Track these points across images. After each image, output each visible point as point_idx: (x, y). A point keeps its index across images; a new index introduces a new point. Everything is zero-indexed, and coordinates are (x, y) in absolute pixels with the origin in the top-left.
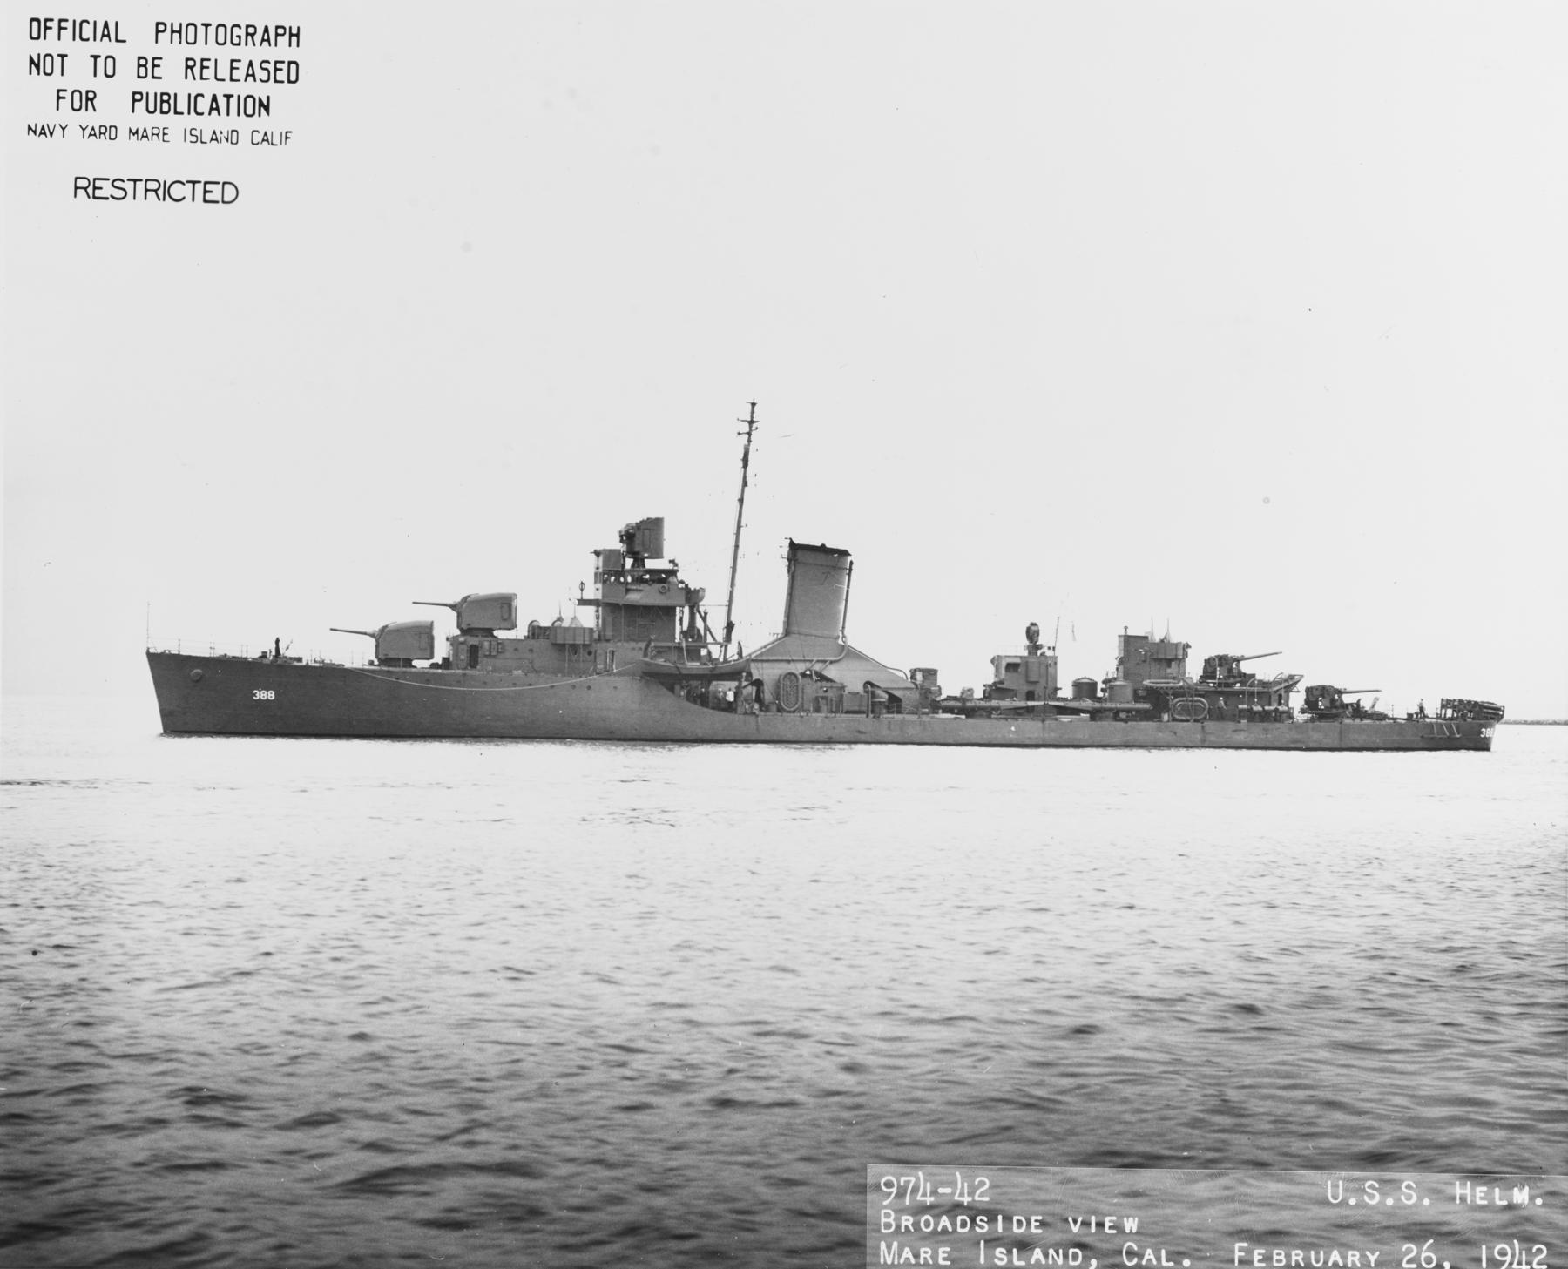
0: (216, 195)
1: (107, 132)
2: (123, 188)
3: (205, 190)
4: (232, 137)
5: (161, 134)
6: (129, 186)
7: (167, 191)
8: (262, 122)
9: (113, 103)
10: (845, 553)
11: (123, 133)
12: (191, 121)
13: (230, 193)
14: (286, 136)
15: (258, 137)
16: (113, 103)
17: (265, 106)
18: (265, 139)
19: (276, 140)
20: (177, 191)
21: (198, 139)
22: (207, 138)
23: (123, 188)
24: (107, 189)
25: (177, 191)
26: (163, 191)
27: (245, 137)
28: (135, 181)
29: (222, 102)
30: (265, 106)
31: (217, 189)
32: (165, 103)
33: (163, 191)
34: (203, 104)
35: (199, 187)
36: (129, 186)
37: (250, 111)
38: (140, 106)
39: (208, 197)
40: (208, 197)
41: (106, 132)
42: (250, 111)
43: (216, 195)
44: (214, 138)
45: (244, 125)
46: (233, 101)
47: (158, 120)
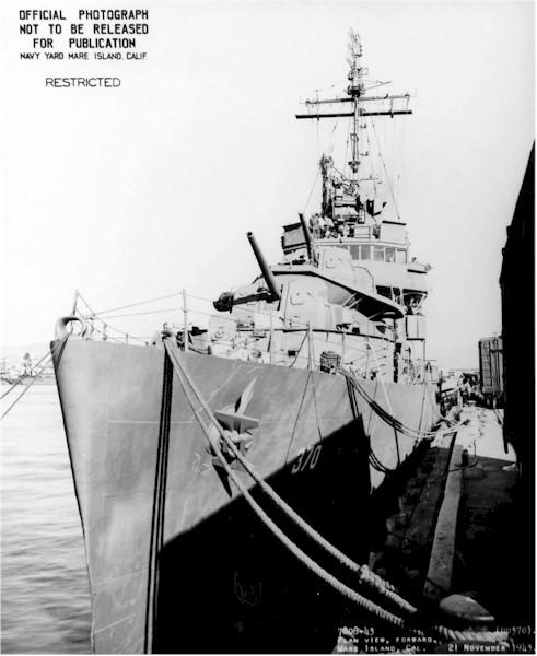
0: (110, 82)
1: (58, 56)
2: (67, 83)
3: (105, 82)
4: (117, 56)
5: (84, 56)
6: (71, 81)
7: (88, 83)
8: (132, 50)
9: (61, 43)
11: (66, 56)
12: (98, 50)
13: (117, 82)
14: (144, 55)
16: (61, 43)
20: (92, 82)
21: (102, 57)
22: (106, 56)
23: (67, 83)
24: (61, 83)
25: (92, 82)
26: (87, 82)
27: (124, 56)
28: (74, 79)
29: (112, 42)
32: (85, 43)
33: (87, 82)
34: (104, 43)
35: (103, 81)
36: (71, 81)
38: (74, 45)
41: (58, 56)
44: (109, 56)
45: (124, 51)
46: (118, 42)
47: (82, 50)
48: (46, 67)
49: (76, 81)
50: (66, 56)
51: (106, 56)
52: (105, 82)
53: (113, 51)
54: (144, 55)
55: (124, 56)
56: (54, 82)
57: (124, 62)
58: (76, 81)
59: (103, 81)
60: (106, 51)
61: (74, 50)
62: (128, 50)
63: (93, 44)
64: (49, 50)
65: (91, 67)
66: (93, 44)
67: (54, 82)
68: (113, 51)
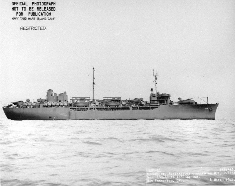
0: (42, 29)
1: (25, 19)
2: (28, 28)
3: (41, 28)
4: (45, 19)
5: (34, 19)
6: (29, 28)
8: (50, 17)
10: (132, 110)
11: (27, 19)
14: (54, 18)
15: (49, 19)
18: (50, 19)
19: (52, 19)
20: (36, 28)
22: (41, 19)
23: (28, 28)
24: (25, 28)
25: (36, 28)
26: (34, 28)
27: (47, 19)
31: (42, 28)
33: (34, 28)
35: (40, 28)
36: (29, 28)
39: (41, 29)
40: (41, 29)
41: (25, 19)
43: (42, 29)
44: (42, 19)
45: (47, 17)
47: (33, 17)
48: (20, 23)
49: (31, 28)
50: (27, 19)
51: (41, 19)
52: (41, 28)
53: (43, 17)
54: (54, 18)
56: (23, 28)
57: (47, 21)
58: (31, 28)
59: (40, 28)
60: (41, 17)
61: (30, 16)
62: (49, 16)
64: (22, 17)
65: (35, 23)
67: (23, 28)
68: (43, 17)
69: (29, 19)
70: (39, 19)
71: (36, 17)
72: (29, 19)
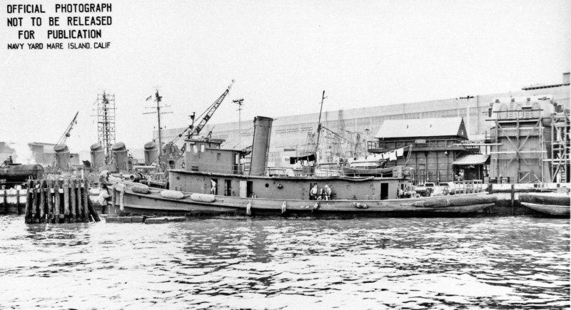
1: (39, 46)
4: (86, 46)
5: (60, 46)
8: (98, 40)
9: (41, 35)
11: (45, 46)
12: (72, 40)
14: (108, 44)
15: (97, 45)
16: (41, 35)
17: (99, 34)
18: (101, 46)
19: (104, 46)
22: (77, 46)
27: (92, 45)
29: (83, 33)
30: (99, 34)
32: (61, 34)
34: (76, 34)
37: (93, 36)
38: (51, 36)
41: (39, 46)
42: (93, 36)
44: (81, 46)
45: (91, 41)
47: (58, 41)
50: (45, 46)
51: (77, 46)
53: (83, 41)
55: (92, 45)
57: (92, 50)
61: (52, 41)
63: (67, 35)
66: (67, 35)
68: (83, 41)
69: (49, 46)
70: (73, 46)
71: (65, 42)
72: (49, 46)
